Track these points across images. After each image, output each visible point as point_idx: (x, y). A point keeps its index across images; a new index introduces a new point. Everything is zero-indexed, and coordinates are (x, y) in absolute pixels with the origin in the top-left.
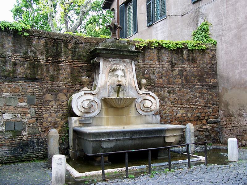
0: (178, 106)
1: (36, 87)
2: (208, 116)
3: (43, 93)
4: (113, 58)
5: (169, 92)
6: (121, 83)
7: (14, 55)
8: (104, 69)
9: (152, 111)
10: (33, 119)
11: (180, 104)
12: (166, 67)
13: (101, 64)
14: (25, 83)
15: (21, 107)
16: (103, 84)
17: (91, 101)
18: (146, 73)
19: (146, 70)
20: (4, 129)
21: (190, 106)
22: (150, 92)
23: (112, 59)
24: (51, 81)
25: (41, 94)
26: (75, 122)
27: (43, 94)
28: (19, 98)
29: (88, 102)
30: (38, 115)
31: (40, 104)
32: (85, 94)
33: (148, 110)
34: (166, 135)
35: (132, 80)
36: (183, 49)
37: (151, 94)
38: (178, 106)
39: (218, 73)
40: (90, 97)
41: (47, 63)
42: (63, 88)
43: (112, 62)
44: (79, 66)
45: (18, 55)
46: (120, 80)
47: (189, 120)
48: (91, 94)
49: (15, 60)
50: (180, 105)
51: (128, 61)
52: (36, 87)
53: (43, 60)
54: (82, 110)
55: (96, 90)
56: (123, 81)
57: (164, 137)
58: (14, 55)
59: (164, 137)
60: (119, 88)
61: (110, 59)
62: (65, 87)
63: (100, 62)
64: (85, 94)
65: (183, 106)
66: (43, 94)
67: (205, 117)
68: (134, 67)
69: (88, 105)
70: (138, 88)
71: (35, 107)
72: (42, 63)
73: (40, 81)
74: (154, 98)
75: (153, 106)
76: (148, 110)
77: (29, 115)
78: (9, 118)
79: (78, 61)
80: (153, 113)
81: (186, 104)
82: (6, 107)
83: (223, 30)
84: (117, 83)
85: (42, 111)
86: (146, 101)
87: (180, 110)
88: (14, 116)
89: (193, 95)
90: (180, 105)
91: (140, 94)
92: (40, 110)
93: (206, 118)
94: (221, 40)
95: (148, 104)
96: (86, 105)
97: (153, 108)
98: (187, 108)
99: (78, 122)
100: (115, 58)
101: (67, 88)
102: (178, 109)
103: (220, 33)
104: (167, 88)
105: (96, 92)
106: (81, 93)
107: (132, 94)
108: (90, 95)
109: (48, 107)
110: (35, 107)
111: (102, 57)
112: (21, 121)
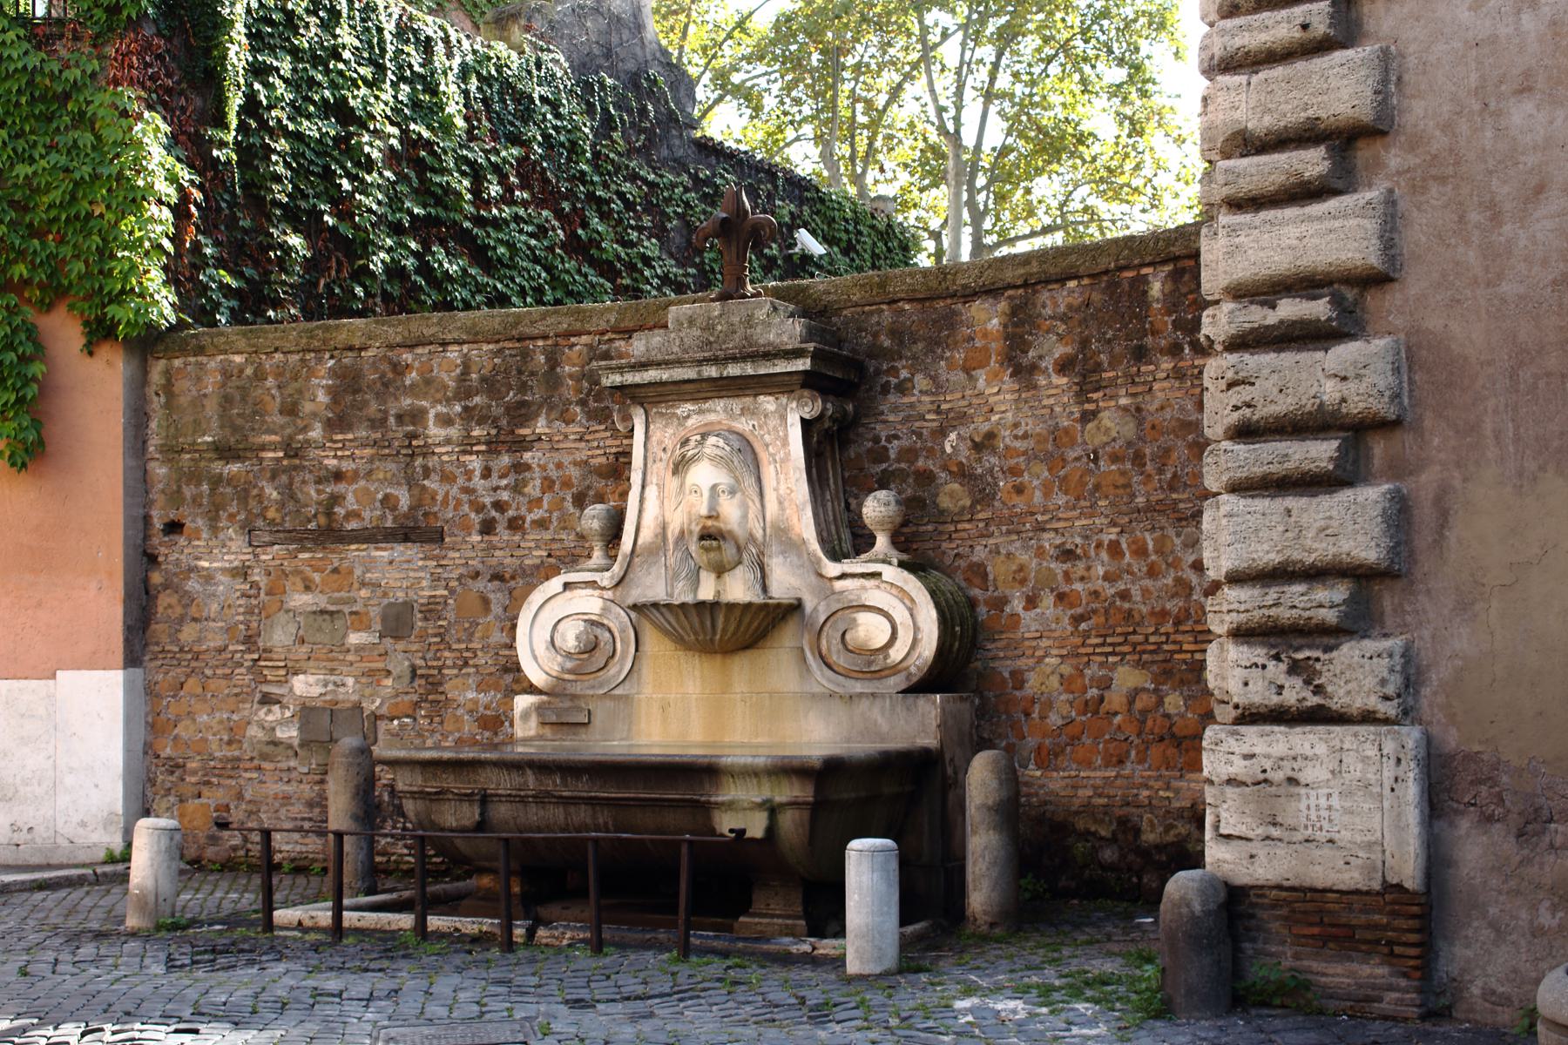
0: (1109, 640)
1: (420, 563)
3: (446, 587)
4: (694, 400)
7: (335, 442)
9: (895, 669)
10: (407, 698)
11: (1119, 630)
12: (1052, 401)
14: (377, 549)
15: (360, 649)
16: (646, 535)
18: (949, 450)
19: (953, 436)
20: (295, 734)
21: (1180, 643)
23: (689, 406)
24: (482, 533)
25: (437, 593)
26: (525, 716)
27: (446, 593)
28: (352, 613)
30: (423, 682)
31: (435, 635)
32: (567, 586)
33: (870, 663)
34: (713, 799)
35: (786, 504)
36: (1144, 271)
38: (1109, 640)
41: (467, 458)
42: (538, 561)
43: (690, 422)
44: (614, 450)
45: (350, 436)
47: (1173, 736)
48: (592, 584)
49: (335, 462)
50: (1120, 639)
51: (768, 403)
52: (420, 563)
53: (448, 441)
58: (335, 442)
59: (705, 809)
61: (686, 408)
62: (549, 556)
63: (632, 430)
65: (1134, 645)
66: (446, 593)
70: (815, 546)
71: (415, 647)
72: (445, 458)
73: (437, 537)
75: (898, 644)
76: (871, 665)
77: (389, 682)
78: (317, 691)
79: (606, 429)
80: (897, 682)
81: (1152, 630)
82: (305, 649)
84: (696, 529)
85: (440, 669)
86: (863, 617)
87: (1120, 669)
88: (331, 687)
90: (1120, 639)
91: (831, 579)
92: (435, 663)
95: (871, 630)
96: (570, 637)
97: (897, 654)
98: (1160, 657)
99: (533, 722)
100: (706, 399)
101: (559, 558)
102: (1111, 659)
104: (1052, 534)
105: (612, 578)
106: (555, 584)
107: (785, 582)
108: (589, 591)
109: (467, 649)
110: (415, 647)
111: (642, 405)
112: (358, 707)
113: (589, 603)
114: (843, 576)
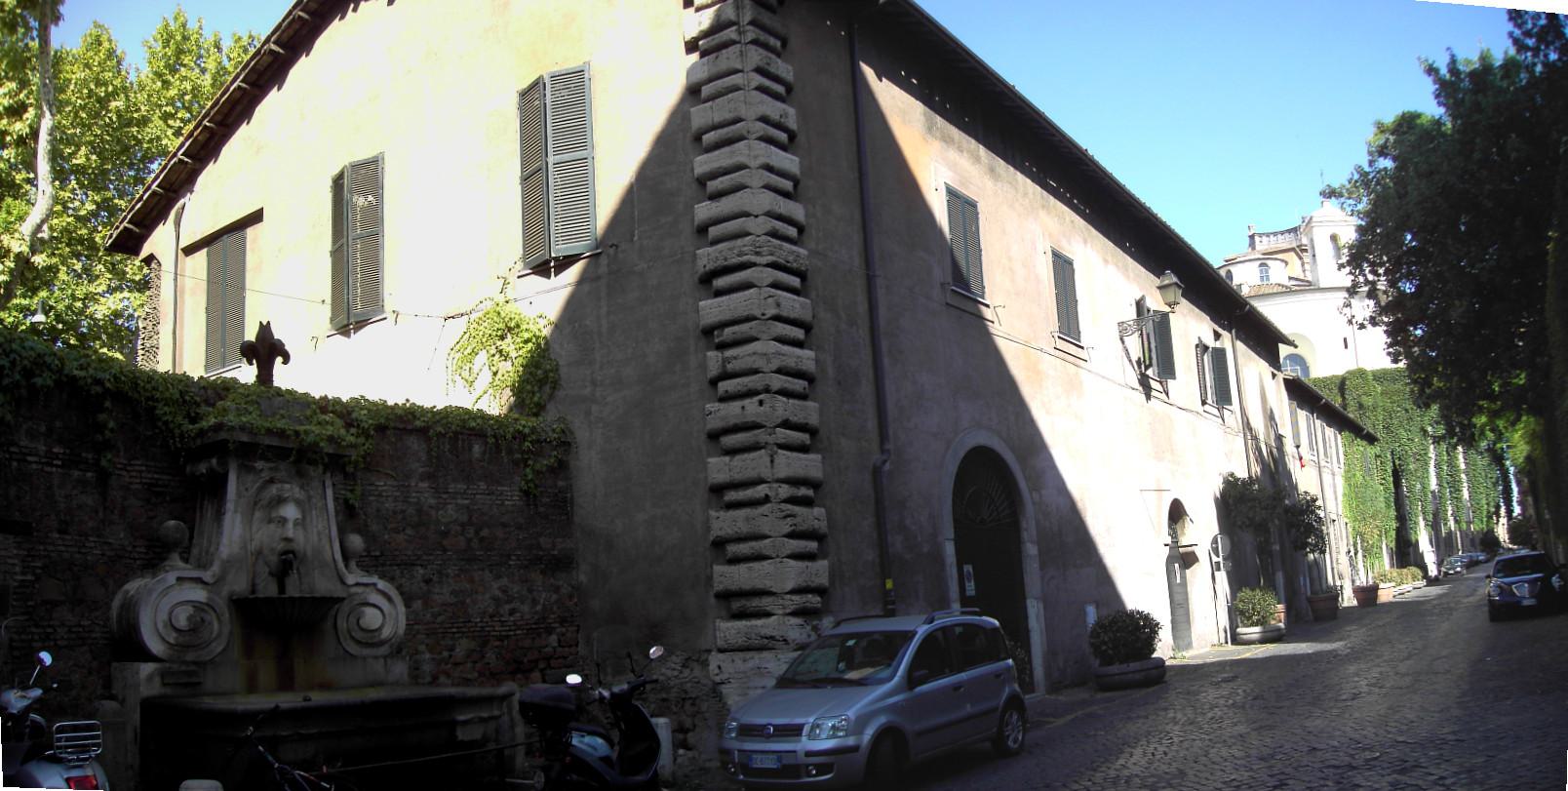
2: (548, 659)
5: (428, 581)
6: (294, 546)
8: (239, 495)
9: (382, 643)
13: (232, 478)
17: (197, 606)
22: (375, 579)
26: (150, 678)
29: (190, 610)
37: (382, 584)
39: (577, 519)
40: (199, 594)
46: (290, 534)
48: (199, 580)
54: (172, 638)
55: (216, 568)
56: (301, 540)
57: (455, 723)
60: (287, 563)
61: (259, 465)
64: (179, 579)
67: (536, 661)
68: (329, 492)
69: (189, 619)
70: (341, 565)
74: (389, 599)
80: (384, 650)
83: (594, 383)
84: (281, 546)
86: (369, 611)
89: (504, 592)
93: (542, 665)
94: (588, 413)
95: (371, 618)
97: (386, 633)
103: (587, 391)
113: (199, 594)
114: (357, 584)
